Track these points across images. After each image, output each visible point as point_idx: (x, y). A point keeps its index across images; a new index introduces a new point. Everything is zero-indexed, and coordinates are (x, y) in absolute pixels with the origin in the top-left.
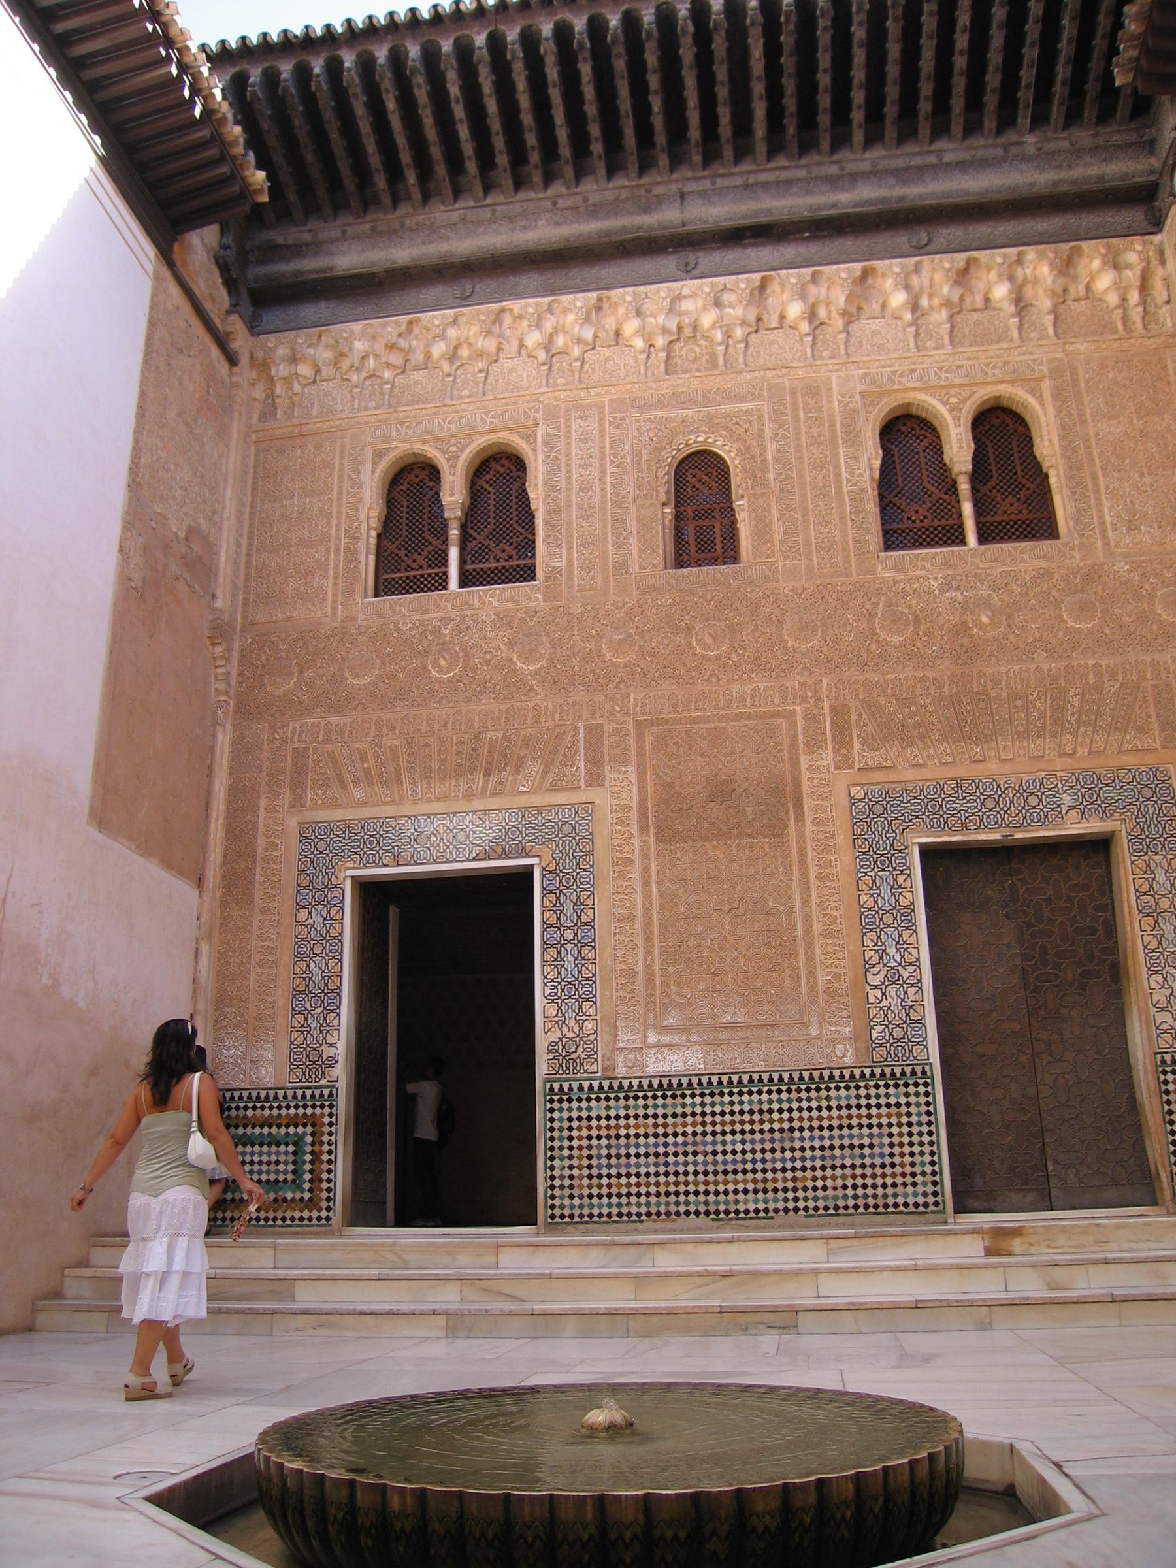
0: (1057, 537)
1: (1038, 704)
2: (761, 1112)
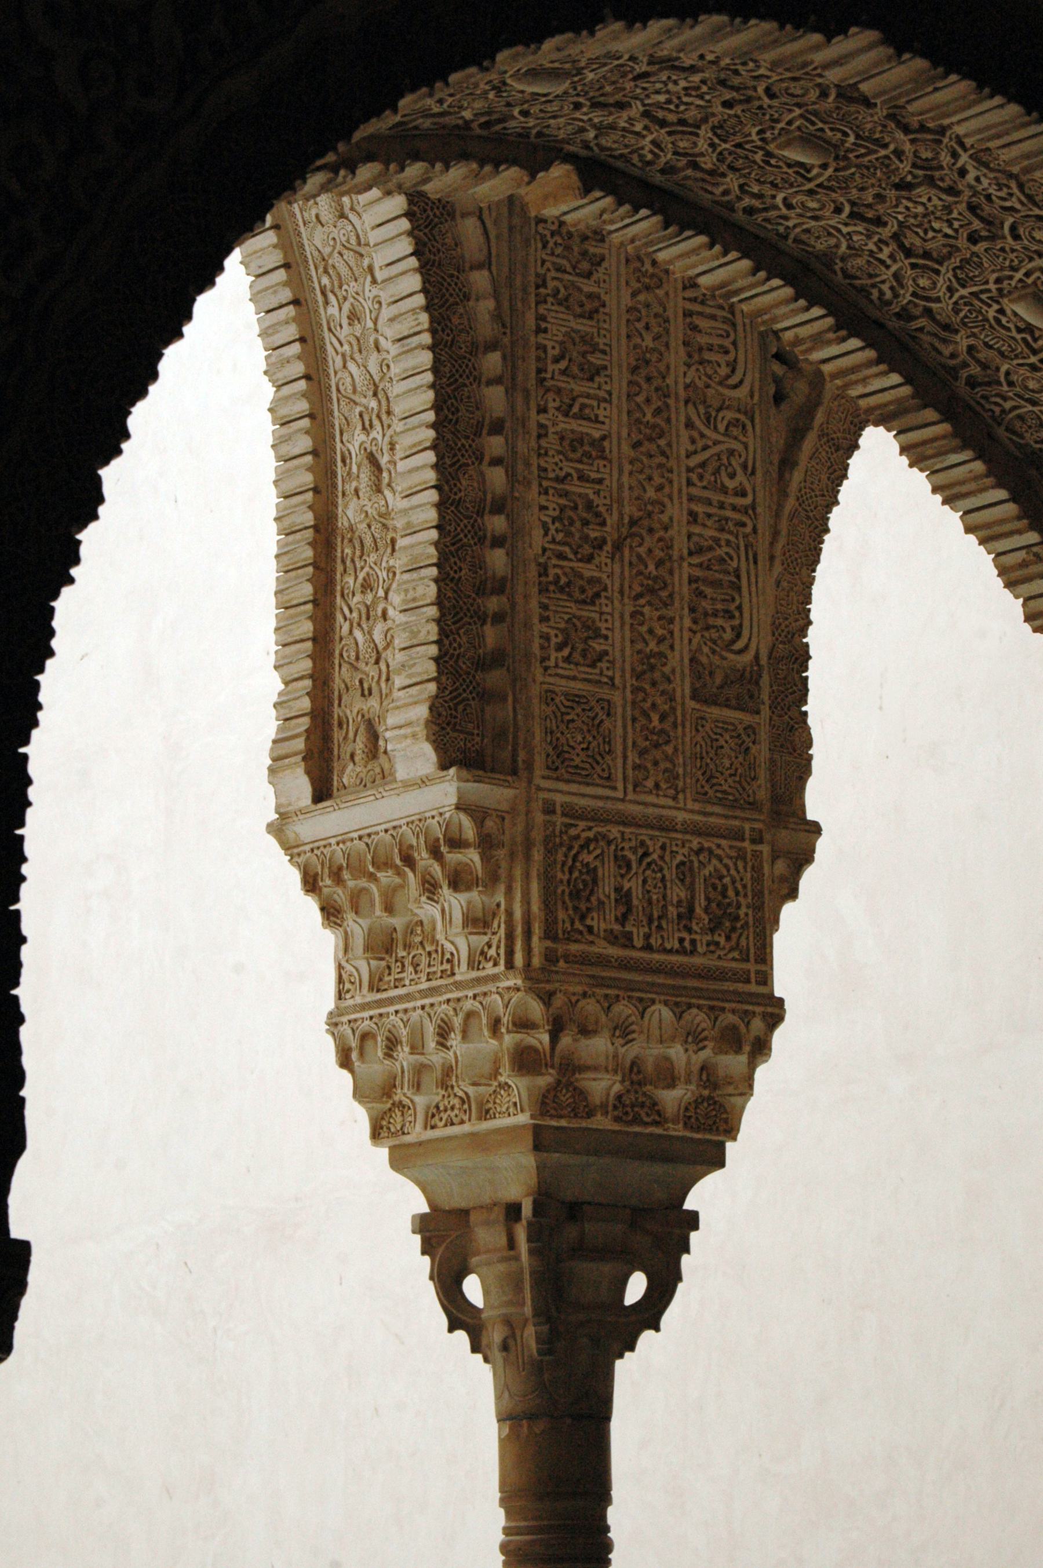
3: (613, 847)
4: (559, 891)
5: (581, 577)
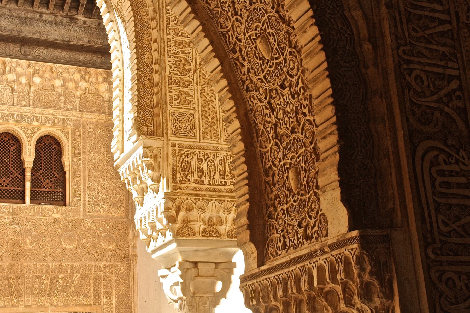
0: (65, 204)
1: (45, 281)
3: (196, 156)
4: (178, 169)
5: (183, 80)
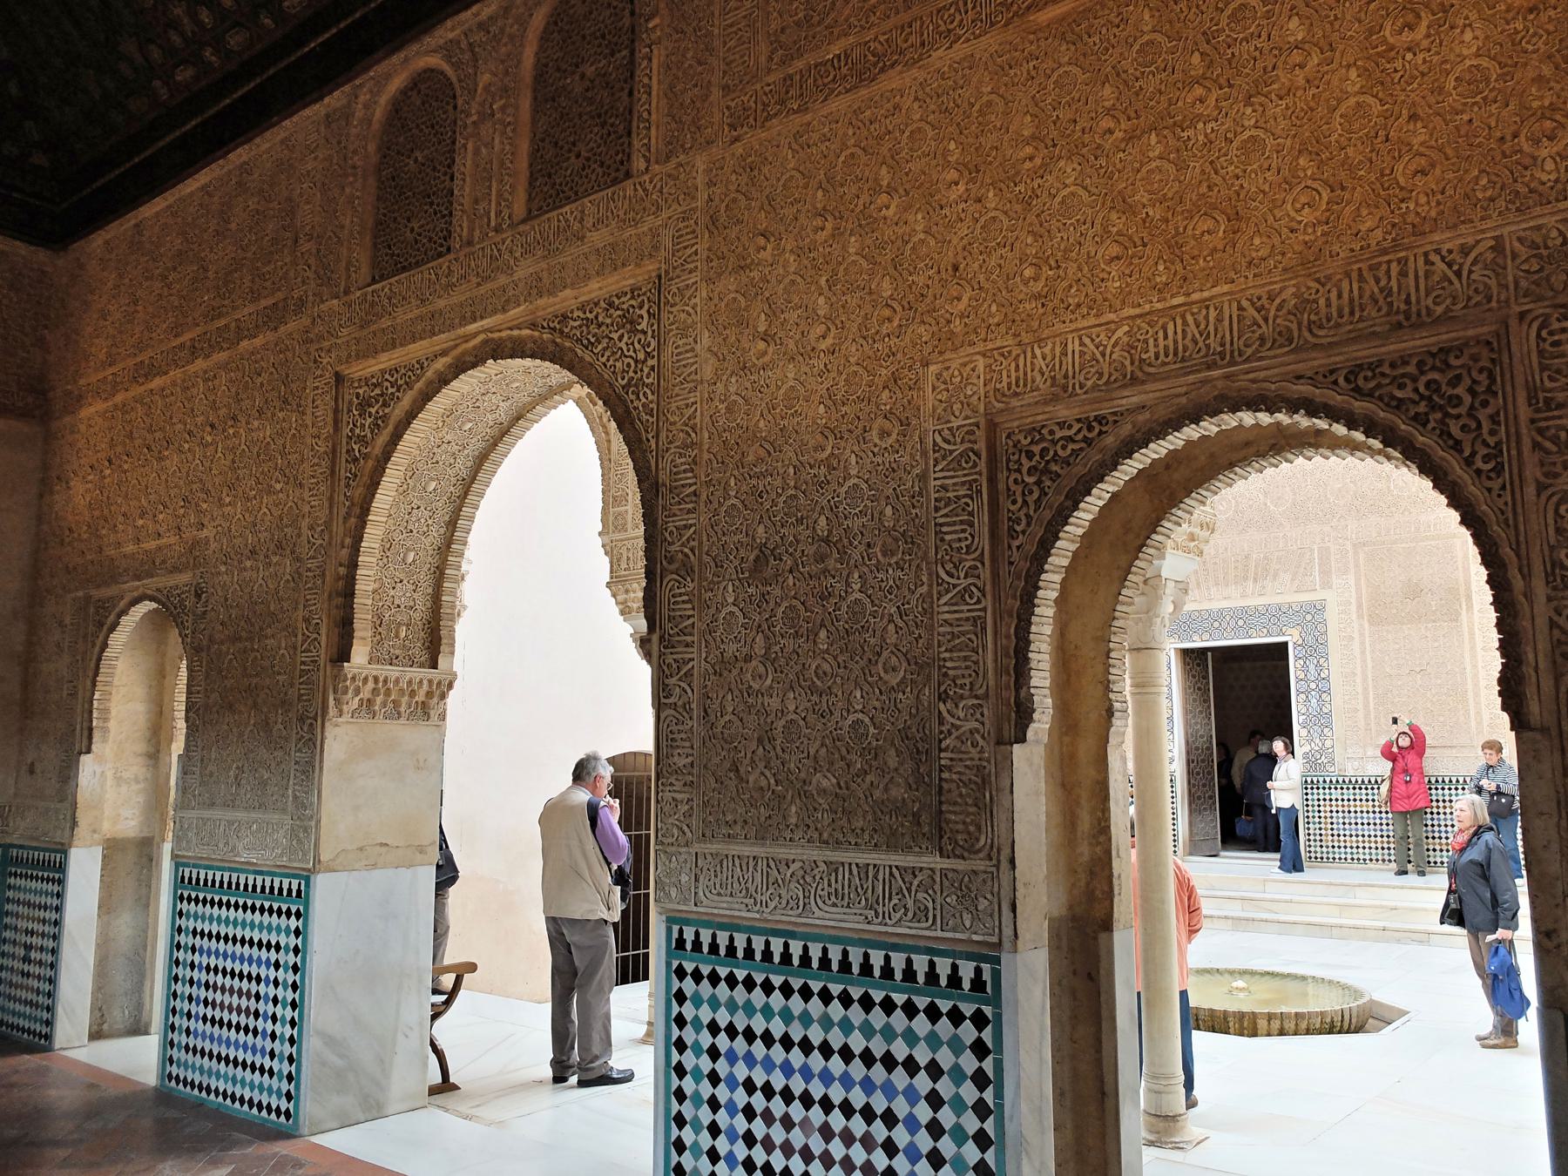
2: (1444, 801)
